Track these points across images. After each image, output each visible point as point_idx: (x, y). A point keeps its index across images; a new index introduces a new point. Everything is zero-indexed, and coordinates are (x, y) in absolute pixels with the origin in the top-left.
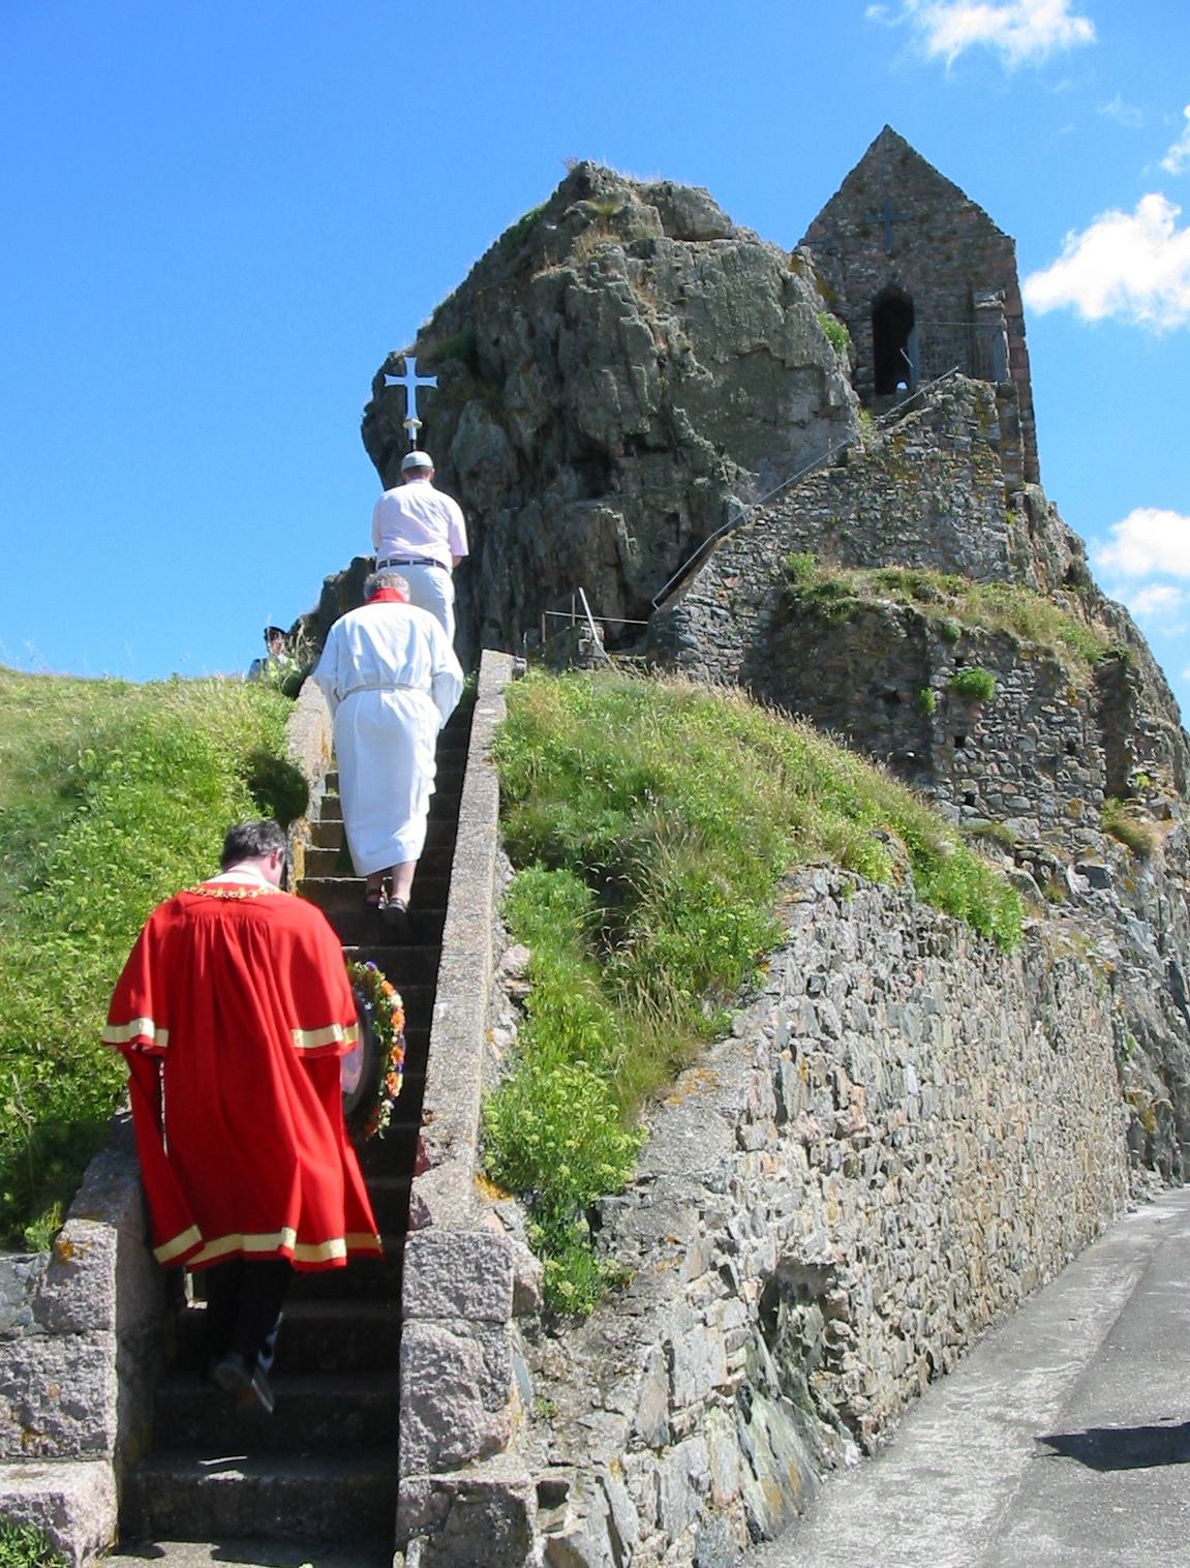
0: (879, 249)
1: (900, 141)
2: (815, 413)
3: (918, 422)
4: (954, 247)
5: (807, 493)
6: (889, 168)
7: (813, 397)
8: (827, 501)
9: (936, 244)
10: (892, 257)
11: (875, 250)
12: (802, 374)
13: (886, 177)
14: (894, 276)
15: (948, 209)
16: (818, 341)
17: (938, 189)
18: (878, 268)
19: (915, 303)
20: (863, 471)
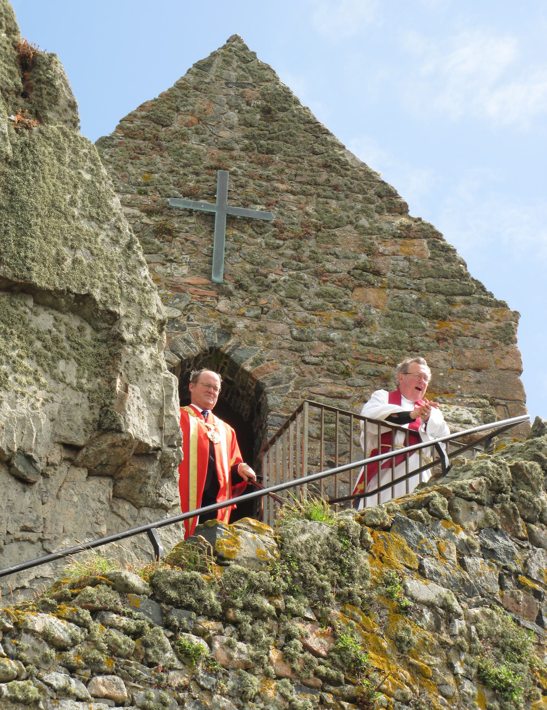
0: (193, 270)
1: (264, 74)
2: (71, 447)
3: (439, 501)
4: (372, 301)
5: (61, 629)
6: (234, 117)
7: (74, 398)
8: (128, 677)
9: (331, 288)
10: (222, 291)
11: (185, 270)
12: (44, 320)
13: (226, 134)
14: (227, 331)
15: (364, 222)
16: (115, 242)
17: (336, 180)
18: (186, 310)
19: (273, 399)
20: (266, 604)
